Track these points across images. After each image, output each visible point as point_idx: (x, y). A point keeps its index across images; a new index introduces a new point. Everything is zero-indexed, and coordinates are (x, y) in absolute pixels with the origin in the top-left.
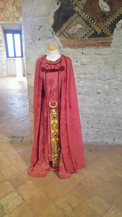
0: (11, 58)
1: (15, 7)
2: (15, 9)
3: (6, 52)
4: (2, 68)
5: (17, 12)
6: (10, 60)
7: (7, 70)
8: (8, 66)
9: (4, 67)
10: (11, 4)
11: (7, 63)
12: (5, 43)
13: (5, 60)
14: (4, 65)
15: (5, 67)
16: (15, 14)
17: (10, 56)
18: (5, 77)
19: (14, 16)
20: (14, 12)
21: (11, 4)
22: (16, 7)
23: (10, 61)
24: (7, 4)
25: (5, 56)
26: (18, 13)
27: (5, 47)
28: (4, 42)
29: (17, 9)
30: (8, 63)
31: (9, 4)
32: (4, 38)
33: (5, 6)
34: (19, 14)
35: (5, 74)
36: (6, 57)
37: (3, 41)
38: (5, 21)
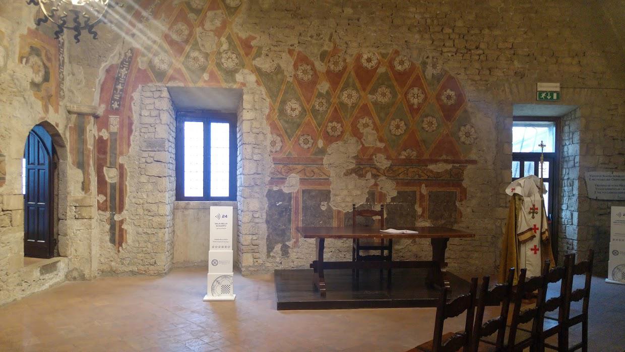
0: (191, 202)
1: (223, 39)
2: (225, 46)
3: (173, 179)
4: (154, 240)
5: (229, 53)
6: (186, 208)
7: (172, 244)
8: (178, 233)
9: (160, 235)
10: (211, 30)
11: (173, 219)
12: (174, 151)
13: (167, 209)
14: (162, 227)
15: (166, 235)
16: (223, 60)
17: (187, 194)
19: (219, 65)
20: (219, 53)
21: (211, 30)
22: (229, 38)
23: (186, 212)
24: (198, 30)
25: (169, 196)
26: (234, 56)
27: (174, 162)
28: (173, 146)
29: (230, 44)
30: (177, 220)
31: (203, 28)
33: (191, 34)
34: (236, 61)
35: (163, 261)
36: (174, 198)
37: (167, 144)
38: (185, 80)
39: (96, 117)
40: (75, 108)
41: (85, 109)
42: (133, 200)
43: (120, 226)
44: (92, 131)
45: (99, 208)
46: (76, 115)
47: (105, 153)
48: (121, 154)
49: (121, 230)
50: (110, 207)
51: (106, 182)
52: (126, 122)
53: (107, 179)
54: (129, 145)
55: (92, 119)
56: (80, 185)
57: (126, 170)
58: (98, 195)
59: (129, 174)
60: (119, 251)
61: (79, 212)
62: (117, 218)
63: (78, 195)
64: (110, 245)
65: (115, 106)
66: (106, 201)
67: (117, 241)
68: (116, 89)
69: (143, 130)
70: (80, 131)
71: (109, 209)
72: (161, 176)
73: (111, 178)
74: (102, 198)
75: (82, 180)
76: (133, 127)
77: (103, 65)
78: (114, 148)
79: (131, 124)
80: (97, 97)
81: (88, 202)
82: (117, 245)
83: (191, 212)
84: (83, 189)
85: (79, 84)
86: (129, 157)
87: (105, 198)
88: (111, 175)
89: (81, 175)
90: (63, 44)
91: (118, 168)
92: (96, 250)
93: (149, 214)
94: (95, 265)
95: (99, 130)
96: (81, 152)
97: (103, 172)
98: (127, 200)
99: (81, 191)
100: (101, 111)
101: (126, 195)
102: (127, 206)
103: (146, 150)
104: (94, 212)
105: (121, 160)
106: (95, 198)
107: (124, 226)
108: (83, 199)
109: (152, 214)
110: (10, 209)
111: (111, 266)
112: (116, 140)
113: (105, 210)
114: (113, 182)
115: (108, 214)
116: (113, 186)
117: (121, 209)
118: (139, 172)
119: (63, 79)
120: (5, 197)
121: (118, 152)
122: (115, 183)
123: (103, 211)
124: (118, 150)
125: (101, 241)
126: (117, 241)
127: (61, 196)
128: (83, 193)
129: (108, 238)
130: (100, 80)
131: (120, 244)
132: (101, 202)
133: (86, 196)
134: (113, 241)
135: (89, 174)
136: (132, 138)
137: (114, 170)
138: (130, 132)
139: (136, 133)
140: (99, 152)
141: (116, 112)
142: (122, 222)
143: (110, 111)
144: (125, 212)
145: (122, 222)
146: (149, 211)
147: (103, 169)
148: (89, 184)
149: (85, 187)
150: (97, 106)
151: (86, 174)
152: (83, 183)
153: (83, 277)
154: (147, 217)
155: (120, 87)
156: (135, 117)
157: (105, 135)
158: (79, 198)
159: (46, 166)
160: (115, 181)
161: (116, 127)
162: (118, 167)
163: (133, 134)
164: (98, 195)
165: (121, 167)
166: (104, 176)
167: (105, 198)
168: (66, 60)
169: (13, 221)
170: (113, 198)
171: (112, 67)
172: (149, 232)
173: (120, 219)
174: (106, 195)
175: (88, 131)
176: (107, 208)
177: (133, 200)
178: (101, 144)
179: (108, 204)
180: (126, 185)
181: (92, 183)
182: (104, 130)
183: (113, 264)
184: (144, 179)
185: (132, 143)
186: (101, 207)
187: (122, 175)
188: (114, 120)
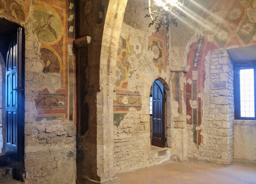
0: (246, 121)
3: (232, 106)
4: (220, 143)
6: (241, 124)
7: (233, 146)
8: (236, 139)
9: (224, 140)
11: (233, 131)
12: (232, 89)
13: (228, 125)
14: (225, 135)
15: (228, 140)
17: (242, 115)
18: (224, 165)
23: (242, 127)
25: (230, 116)
27: (233, 95)
28: (232, 85)
30: (236, 132)
32: (232, 79)
35: (226, 157)
36: (233, 118)
37: (227, 85)
39: (185, 73)
40: (174, 69)
41: (179, 69)
42: (207, 119)
43: (199, 133)
44: (183, 80)
45: (187, 123)
46: (175, 73)
47: (190, 92)
48: (199, 92)
49: (200, 136)
50: (193, 122)
51: (191, 108)
52: (202, 73)
53: (192, 106)
54: (204, 87)
55: (183, 74)
56: (177, 110)
57: (202, 101)
58: (187, 115)
59: (204, 103)
60: (198, 148)
61: (177, 125)
62: (197, 128)
63: (176, 115)
64: (193, 143)
65: (195, 65)
66: (191, 118)
67: (197, 142)
68: (195, 56)
69: (212, 77)
70: (177, 80)
71: (193, 124)
72: (224, 104)
73: (194, 106)
74: (189, 117)
75: (178, 107)
76: (206, 76)
77: (188, 44)
78: (195, 89)
79: (204, 74)
80: (185, 61)
81: (181, 119)
82: (197, 144)
83: (246, 127)
84: (179, 112)
85: (176, 56)
86: (204, 94)
87: (190, 117)
88: (194, 104)
89: (178, 105)
90: (168, 37)
91: (198, 100)
92: (185, 146)
93: (217, 127)
94: (185, 154)
95: (187, 79)
96: (177, 92)
97: (189, 102)
98: (203, 119)
99: (177, 112)
100: (187, 69)
101: (202, 116)
102: (203, 122)
103: (214, 89)
104: (185, 124)
105: (199, 95)
106: (185, 117)
107: (202, 134)
108: (179, 117)
109: (219, 127)
110: (144, 122)
111: (194, 156)
112: (196, 84)
113: (190, 124)
114: (195, 108)
115: (192, 126)
116: (195, 110)
117: (200, 123)
118: (210, 102)
119: (168, 55)
120: (142, 116)
121: (197, 91)
122: (196, 109)
123: (189, 124)
124: (197, 90)
125: (189, 141)
126: (197, 142)
127: (168, 115)
128: (179, 114)
129: (192, 140)
130: (187, 52)
131: (199, 144)
132: (189, 119)
133: (180, 115)
134: (195, 141)
135: (181, 104)
136: (205, 82)
137: (196, 101)
138: (204, 79)
139: (208, 80)
140: (187, 91)
141: (196, 69)
142: (200, 131)
143: (193, 68)
144: (202, 125)
145: (200, 131)
146: (217, 125)
147: (189, 101)
148: (182, 109)
149: (180, 111)
150: (186, 66)
151: (180, 103)
152: (179, 109)
153: (179, 160)
154: (215, 129)
155: (197, 54)
156: (207, 70)
157: (190, 82)
158: (177, 117)
159: (161, 101)
160: (196, 108)
161: (196, 77)
162: (197, 99)
163: (206, 80)
164: (187, 115)
165: (199, 99)
166: (190, 104)
167: (190, 117)
168: (170, 45)
169: (145, 127)
170: (195, 117)
171: (193, 44)
172: (217, 137)
173: (199, 129)
174: (191, 115)
175: (181, 80)
176: (191, 123)
177: (207, 119)
178: (188, 87)
179: (192, 120)
180: (202, 110)
181: (183, 108)
182: (189, 79)
183: (195, 154)
184: (213, 106)
185: (205, 85)
186: (189, 122)
187: (200, 104)
188: (195, 74)
